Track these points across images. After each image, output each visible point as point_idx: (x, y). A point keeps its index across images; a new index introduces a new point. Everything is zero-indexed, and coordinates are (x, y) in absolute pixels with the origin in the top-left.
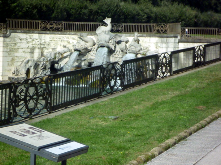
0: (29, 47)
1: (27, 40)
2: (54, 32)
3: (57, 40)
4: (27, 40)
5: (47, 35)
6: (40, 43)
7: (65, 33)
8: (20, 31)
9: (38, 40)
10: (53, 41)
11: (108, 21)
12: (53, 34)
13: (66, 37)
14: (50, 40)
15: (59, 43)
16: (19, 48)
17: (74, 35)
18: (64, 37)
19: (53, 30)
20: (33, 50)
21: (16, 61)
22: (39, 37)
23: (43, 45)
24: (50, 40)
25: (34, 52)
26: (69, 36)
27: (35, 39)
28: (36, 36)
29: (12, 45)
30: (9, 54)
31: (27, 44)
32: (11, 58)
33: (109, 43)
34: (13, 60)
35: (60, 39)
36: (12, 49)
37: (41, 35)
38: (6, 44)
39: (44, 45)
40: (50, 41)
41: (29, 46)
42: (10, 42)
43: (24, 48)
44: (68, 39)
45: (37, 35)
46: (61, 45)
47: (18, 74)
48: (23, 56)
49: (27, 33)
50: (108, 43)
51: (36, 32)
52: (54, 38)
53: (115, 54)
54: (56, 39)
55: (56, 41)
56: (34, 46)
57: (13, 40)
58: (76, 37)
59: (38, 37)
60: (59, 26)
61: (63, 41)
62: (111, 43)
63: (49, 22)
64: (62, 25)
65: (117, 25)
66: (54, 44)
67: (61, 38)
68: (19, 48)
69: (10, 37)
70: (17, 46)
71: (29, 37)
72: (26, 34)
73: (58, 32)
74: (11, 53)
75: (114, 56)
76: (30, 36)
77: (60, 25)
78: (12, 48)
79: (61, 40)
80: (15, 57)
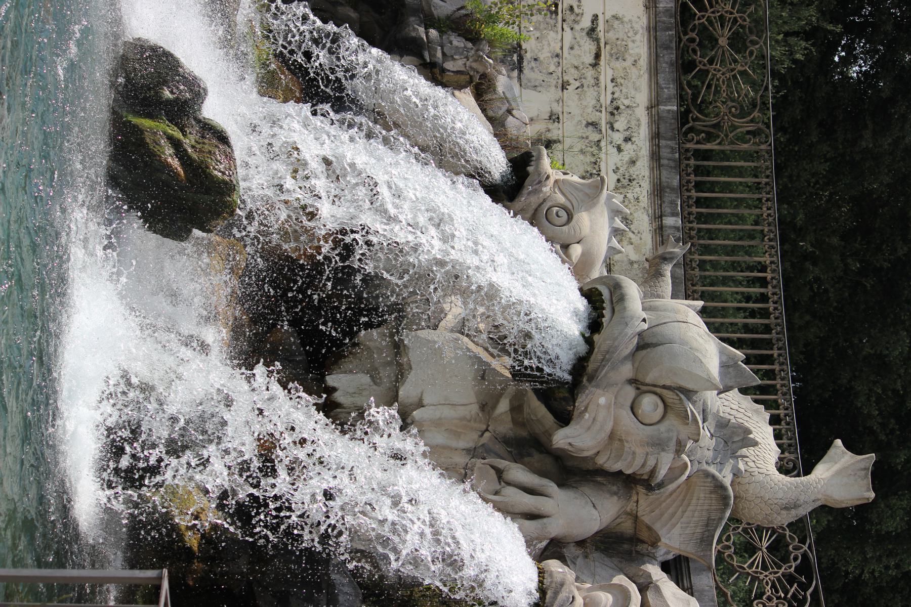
2: (670, 56)
3: (597, 84)
7: (665, 153)
10: (588, 47)
11: (840, 476)
12: (656, 47)
13: (633, 162)
14: (595, 18)
15: (578, 107)
17: (660, 231)
18: (627, 147)
24: (595, 18)
26: (643, 190)
33: (630, 391)
35: (615, 111)
40: (586, 23)
44: (610, 180)
46: (554, 118)
50: (627, 370)
52: (619, 55)
53: (499, 473)
54: (606, 72)
55: (590, 73)
58: (637, 249)
61: (595, 137)
62: (632, 409)
65: (804, 587)
73: (670, 90)
75: (479, 462)
77: (742, 115)
79: (603, 118)
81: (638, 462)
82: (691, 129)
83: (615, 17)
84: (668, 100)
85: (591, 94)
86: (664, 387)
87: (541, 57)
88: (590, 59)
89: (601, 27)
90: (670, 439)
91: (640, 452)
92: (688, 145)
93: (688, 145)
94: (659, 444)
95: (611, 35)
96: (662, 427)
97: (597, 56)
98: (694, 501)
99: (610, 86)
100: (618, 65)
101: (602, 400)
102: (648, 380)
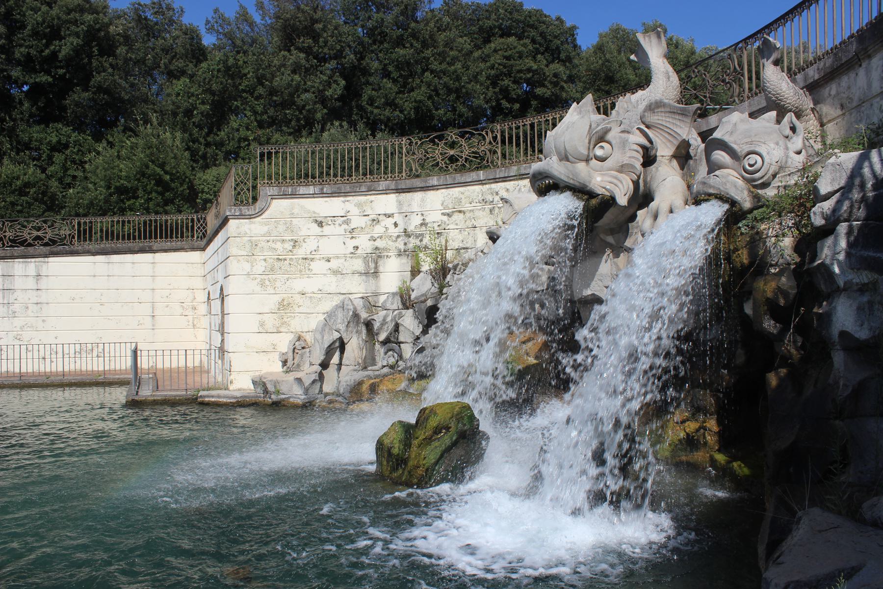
0: (359, 251)
1: (347, 222)
3: (472, 211)
4: (347, 222)
5: (431, 194)
6: (405, 231)
8: (311, 190)
9: (397, 218)
10: (457, 217)
14: (442, 214)
16: (312, 260)
19: (462, 169)
20: (376, 263)
21: (297, 310)
22: (400, 203)
23: (417, 237)
24: (442, 214)
25: (381, 269)
27: (381, 218)
28: (386, 203)
29: (279, 245)
30: (262, 284)
31: (348, 241)
32: (277, 298)
34: (284, 306)
36: (277, 264)
37: (408, 196)
38: (248, 246)
39: (421, 236)
40: (445, 218)
41: (357, 248)
42: (269, 234)
43: (338, 257)
45: (392, 198)
47: (298, 365)
48: (333, 289)
49: (346, 194)
51: (383, 185)
52: (459, 201)
54: (467, 207)
55: (468, 215)
56: (379, 243)
57: (281, 228)
59: (395, 204)
60: (484, 148)
61: (497, 210)
63: (441, 138)
64: (495, 138)
66: (461, 230)
67: (489, 198)
68: (312, 260)
69: (263, 216)
70: (301, 252)
71: (355, 211)
72: (342, 199)
73: (473, 176)
74: (275, 280)
76: (359, 205)
77: (484, 139)
78: (278, 259)
80: (298, 298)
81: (635, 154)
82: (492, 162)
83: (442, 204)
84: (478, 175)
85: (477, 213)
86: (589, 143)
87: (461, 238)
88: (461, 215)
89: (447, 211)
90: (620, 137)
91: (629, 154)
92: (499, 163)
93: (499, 163)
94: (624, 143)
95: (450, 207)
96: (613, 142)
97: (460, 212)
98: (660, 122)
99: (473, 204)
100: (463, 201)
101: (599, 179)
102: (586, 153)
